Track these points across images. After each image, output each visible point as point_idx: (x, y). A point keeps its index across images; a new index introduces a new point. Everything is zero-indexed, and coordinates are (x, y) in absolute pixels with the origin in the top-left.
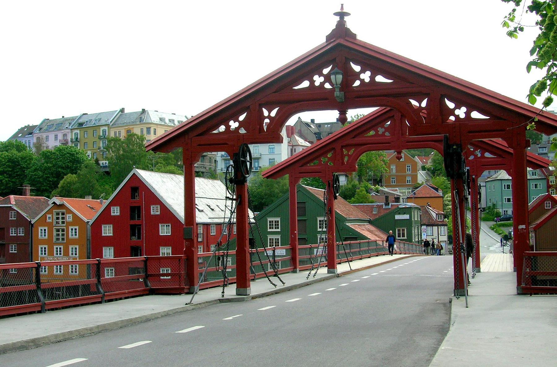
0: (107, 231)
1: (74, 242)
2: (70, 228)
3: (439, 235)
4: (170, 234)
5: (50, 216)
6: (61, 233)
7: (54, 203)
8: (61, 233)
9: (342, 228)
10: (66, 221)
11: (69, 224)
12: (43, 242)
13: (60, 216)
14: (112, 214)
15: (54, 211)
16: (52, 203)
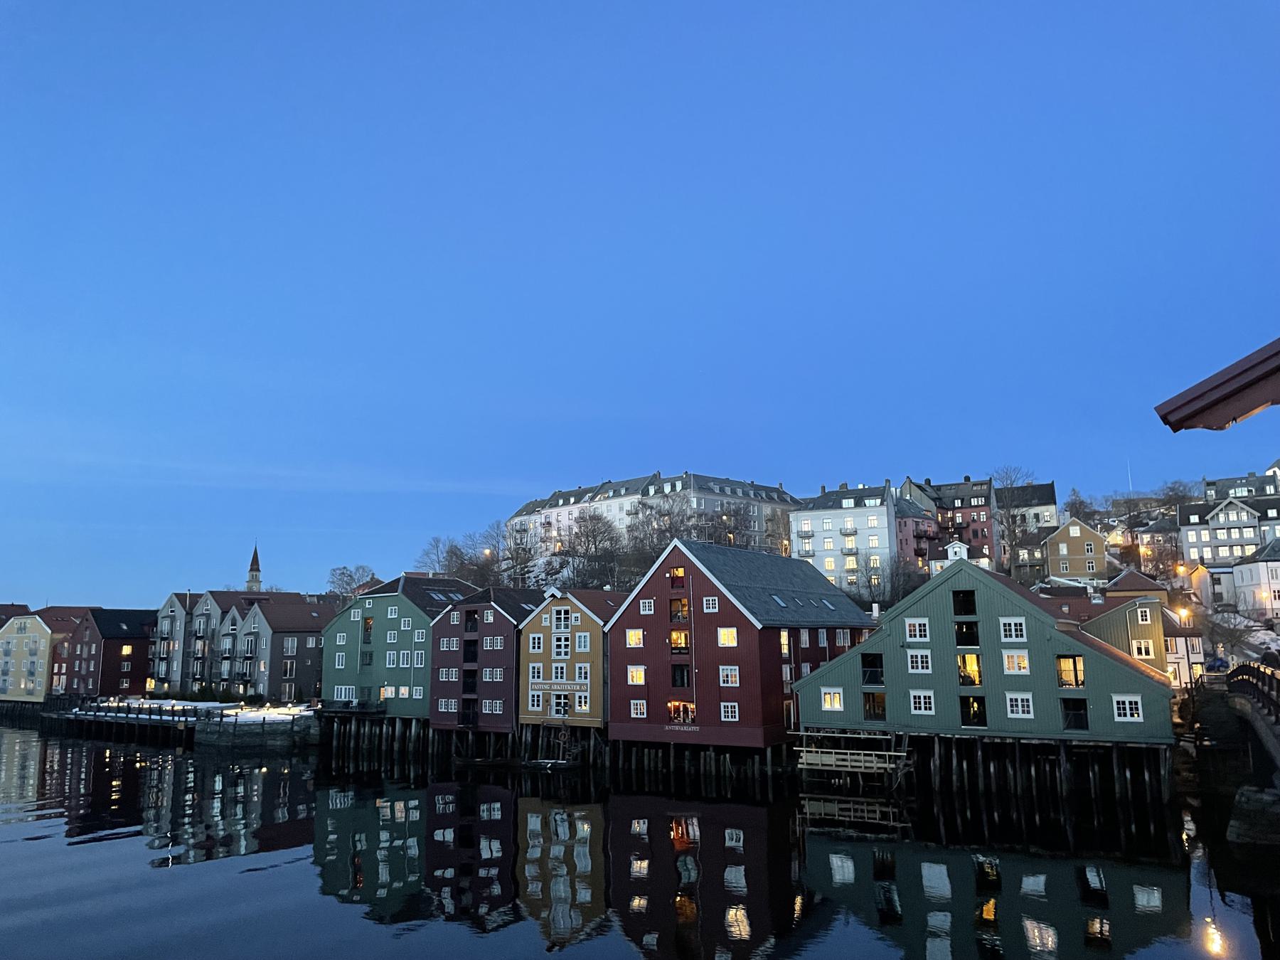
2: (578, 634)
3: (1190, 652)
5: (544, 616)
6: (563, 643)
7: (553, 596)
8: (563, 643)
9: (1049, 638)
10: (571, 625)
11: (576, 629)
12: (536, 658)
14: (642, 613)
16: (551, 596)
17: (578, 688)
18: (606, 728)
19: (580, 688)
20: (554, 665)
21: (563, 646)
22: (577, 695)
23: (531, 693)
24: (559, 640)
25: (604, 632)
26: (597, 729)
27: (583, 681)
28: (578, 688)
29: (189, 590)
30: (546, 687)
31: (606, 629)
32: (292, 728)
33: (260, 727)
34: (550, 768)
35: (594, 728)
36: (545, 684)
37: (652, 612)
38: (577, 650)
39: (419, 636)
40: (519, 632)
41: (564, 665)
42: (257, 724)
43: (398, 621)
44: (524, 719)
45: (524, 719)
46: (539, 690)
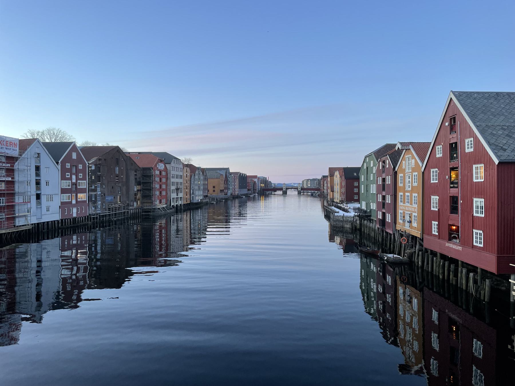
4: (483, 180)
18: (423, 238)
22: (414, 214)
23: (400, 211)
26: (420, 239)
31: (423, 170)
32: (354, 219)
33: (342, 218)
34: (386, 260)
35: (418, 238)
36: (404, 206)
40: (396, 173)
42: (341, 217)
43: (372, 167)
44: (398, 227)
45: (398, 227)
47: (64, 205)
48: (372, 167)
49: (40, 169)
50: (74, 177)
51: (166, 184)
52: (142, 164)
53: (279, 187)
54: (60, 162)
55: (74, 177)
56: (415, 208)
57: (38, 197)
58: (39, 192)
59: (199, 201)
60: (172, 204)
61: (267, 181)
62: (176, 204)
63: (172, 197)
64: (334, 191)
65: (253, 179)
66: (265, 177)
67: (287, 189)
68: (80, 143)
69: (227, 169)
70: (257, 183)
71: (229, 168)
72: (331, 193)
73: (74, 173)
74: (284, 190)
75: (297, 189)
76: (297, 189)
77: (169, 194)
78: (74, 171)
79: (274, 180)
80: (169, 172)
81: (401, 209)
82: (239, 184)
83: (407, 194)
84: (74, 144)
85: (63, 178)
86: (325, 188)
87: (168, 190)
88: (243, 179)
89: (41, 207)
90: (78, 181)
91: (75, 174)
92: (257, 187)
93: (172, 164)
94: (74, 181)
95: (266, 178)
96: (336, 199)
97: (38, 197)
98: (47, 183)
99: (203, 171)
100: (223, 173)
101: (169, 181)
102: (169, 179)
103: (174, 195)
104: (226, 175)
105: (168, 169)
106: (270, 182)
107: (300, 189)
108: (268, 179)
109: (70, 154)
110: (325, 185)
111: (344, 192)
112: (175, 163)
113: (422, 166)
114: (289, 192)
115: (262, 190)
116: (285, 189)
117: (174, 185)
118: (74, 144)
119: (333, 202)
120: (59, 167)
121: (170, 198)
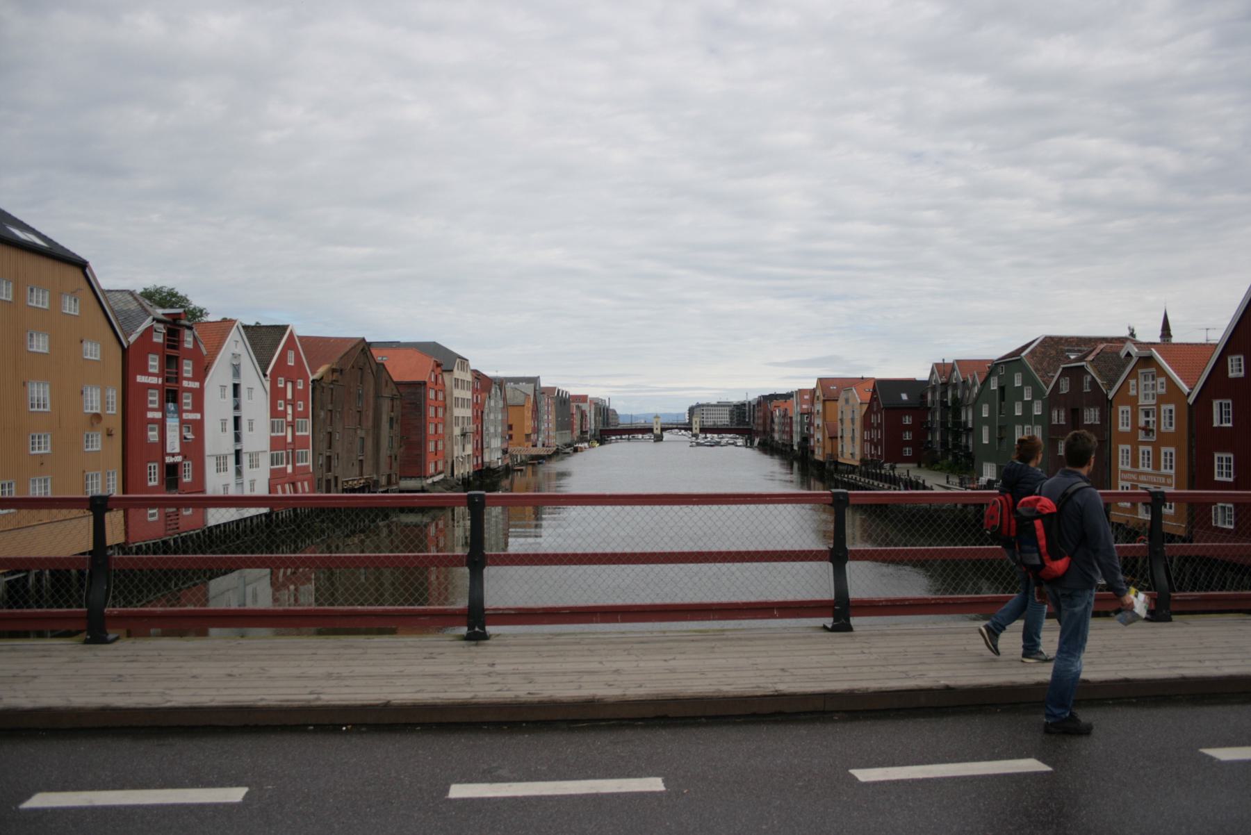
0: (1220, 415)
1: (1164, 439)
5: (1132, 382)
8: (1151, 419)
12: (1126, 438)
13: (1150, 382)
14: (1231, 375)
15: (1140, 371)
17: (1164, 481)
19: (1166, 481)
20: (1141, 448)
21: (1151, 422)
24: (1147, 414)
25: (1188, 404)
27: (1168, 471)
28: (1164, 481)
29: (943, 360)
30: (1134, 477)
31: (1191, 400)
37: (1242, 374)
38: (1163, 428)
39: (1037, 410)
40: (1111, 401)
41: (1150, 448)
43: (1021, 389)
46: (1127, 480)
47: (276, 477)
48: (1021, 389)
49: (240, 392)
50: (290, 411)
51: (443, 421)
52: (401, 370)
53: (641, 423)
54: (268, 373)
55: (290, 411)
56: (1170, 476)
57: (238, 454)
58: (238, 448)
59: (500, 464)
60: (456, 473)
61: (607, 410)
62: (462, 471)
63: (456, 455)
64: (837, 438)
65: (580, 404)
66: (603, 399)
67: (663, 430)
68: (302, 329)
69: (534, 381)
70: (588, 415)
71: (539, 377)
72: (828, 443)
73: (289, 400)
74: (655, 431)
75: (691, 429)
76: (691, 429)
77: (448, 447)
78: (289, 396)
79: (626, 408)
80: (447, 393)
81: (1123, 480)
82: (557, 417)
83: (1141, 448)
84: (291, 331)
85: (274, 413)
86: (776, 428)
87: (447, 437)
88: (564, 403)
89: (242, 483)
90: (297, 420)
91: (292, 403)
92: (589, 426)
93: (457, 374)
94: (290, 418)
95: (605, 401)
96: (847, 455)
97: (238, 454)
98: (251, 422)
99: (501, 383)
100: (528, 388)
101: (448, 415)
102: (448, 409)
103: (457, 451)
104: (535, 395)
105: (446, 384)
106: (614, 411)
107: (698, 429)
108: (607, 404)
109: (284, 354)
110: (776, 420)
111: (878, 439)
112: (460, 368)
113: (1189, 394)
114: (666, 435)
115: (598, 433)
116: (659, 429)
117: (458, 425)
118: (291, 331)
119: (837, 463)
120: (268, 385)
121: (453, 457)
